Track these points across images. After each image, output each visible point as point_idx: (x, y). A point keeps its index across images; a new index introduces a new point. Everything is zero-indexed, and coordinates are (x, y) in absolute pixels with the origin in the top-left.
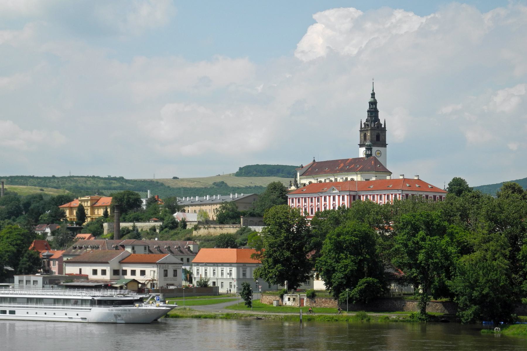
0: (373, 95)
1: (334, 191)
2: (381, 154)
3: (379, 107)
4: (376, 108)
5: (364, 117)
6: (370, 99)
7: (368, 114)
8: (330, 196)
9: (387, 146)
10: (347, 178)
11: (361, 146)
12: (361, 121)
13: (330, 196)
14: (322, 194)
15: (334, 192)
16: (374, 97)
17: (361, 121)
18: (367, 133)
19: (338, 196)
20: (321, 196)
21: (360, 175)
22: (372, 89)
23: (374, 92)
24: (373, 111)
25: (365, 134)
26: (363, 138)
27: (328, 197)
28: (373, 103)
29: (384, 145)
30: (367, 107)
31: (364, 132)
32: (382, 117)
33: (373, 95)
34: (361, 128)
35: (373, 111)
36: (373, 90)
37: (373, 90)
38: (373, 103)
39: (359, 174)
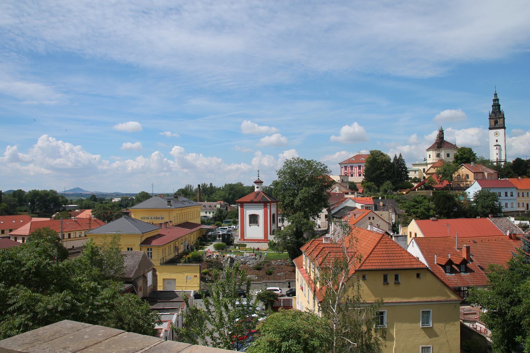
0: (496, 95)
3: (500, 103)
7: (493, 108)
11: (490, 129)
18: (498, 120)
24: (496, 106)
25: (497, 120)
26: (493, 124)
28: (498, 100)
30: (492, 103)
33: (496, 95)
35: (496, 106)
38: (496, 100)
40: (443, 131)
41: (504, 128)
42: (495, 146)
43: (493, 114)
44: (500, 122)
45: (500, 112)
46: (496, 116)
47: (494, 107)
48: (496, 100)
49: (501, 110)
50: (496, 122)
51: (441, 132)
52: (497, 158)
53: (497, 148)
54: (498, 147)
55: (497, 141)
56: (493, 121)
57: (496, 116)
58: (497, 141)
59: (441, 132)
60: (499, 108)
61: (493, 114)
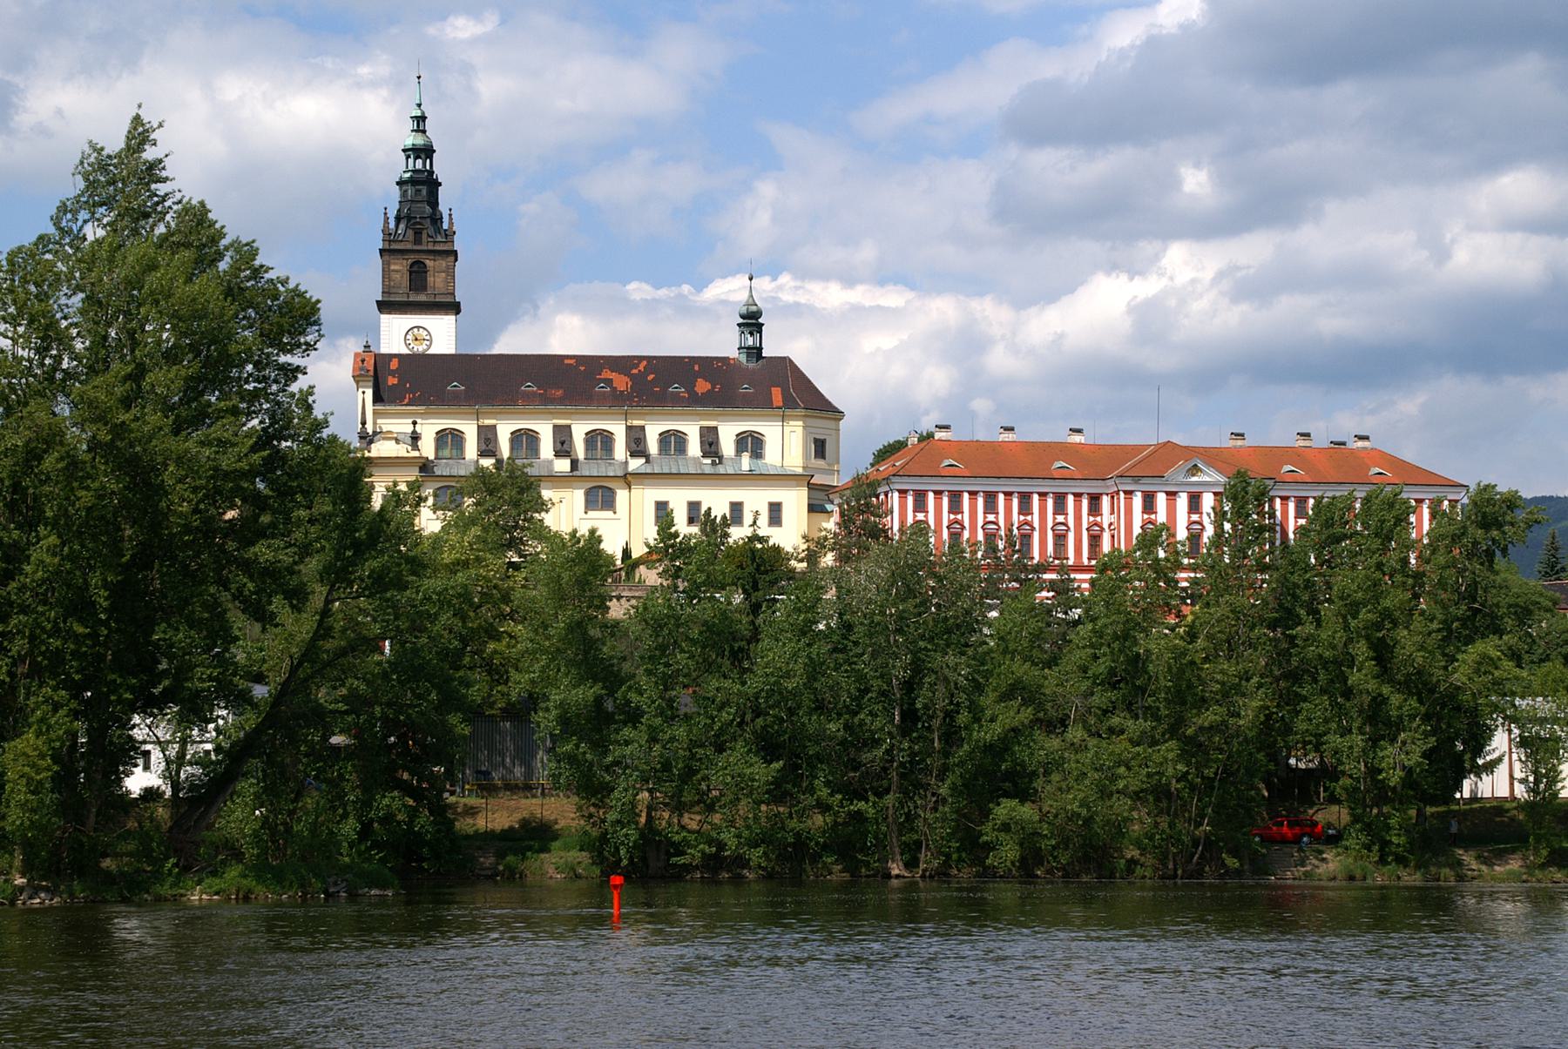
1: (1193, 475)
2: (431, 341)
4: (431, 172)
7: (404, 194)
8: (1172, 495)
10: (715, 429)
11: (385, 306)
12: (385, 214)
13: (1172, 495)
14: (1136, 483)
15: (1194, 479)
16: (424, 132)
19: (1168, 493)
20: (1129, 493)
21: (801, 423)
23: (423, 113)
27: (1161, 499)
28: (426, 152)
30: (400, 167)
31: (412, 258)
33: (421, 119)
37: (419, 105)
39: (796, 418)
41: (454, 308)
43: (402, 226)
44: (436, 280)
45: (436, 219)
46: (418, 241)
47: (410, 190)
49: (443, 207)
50: (418, 275)
56: (400, 266)
57: (418, 241)
60: (434, 203)
61: (402, 226)
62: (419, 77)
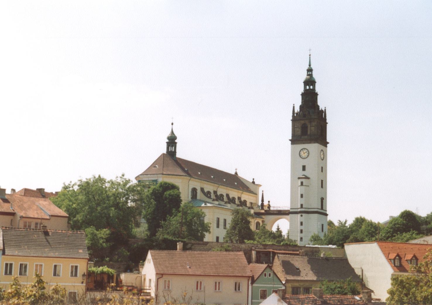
0: (310, 70)
3: (318, 90)
4: (314, 89)
5: (298, 102)
6: (304, 76)
9: (328, 145)
12: (294, 107)
17: (294, 107)
22: (308, 64)
29: (325, 143)
30: (301, 89)
31: (303, 122)
32: (322, 103)
33: (310, 70)
34: (293, 116)
36: (310, 65)
37: (310, 65)
40: (175, 138)
42: (299, 178)
48: (310, 82)
50: (304, 129)
51: (172, 141)
52: (302, 205)
53: (302, 183)
54: (303, 180)
55: (304, 168)
58: (304, 168)
59: (172, 141)
62: (310, 55)
